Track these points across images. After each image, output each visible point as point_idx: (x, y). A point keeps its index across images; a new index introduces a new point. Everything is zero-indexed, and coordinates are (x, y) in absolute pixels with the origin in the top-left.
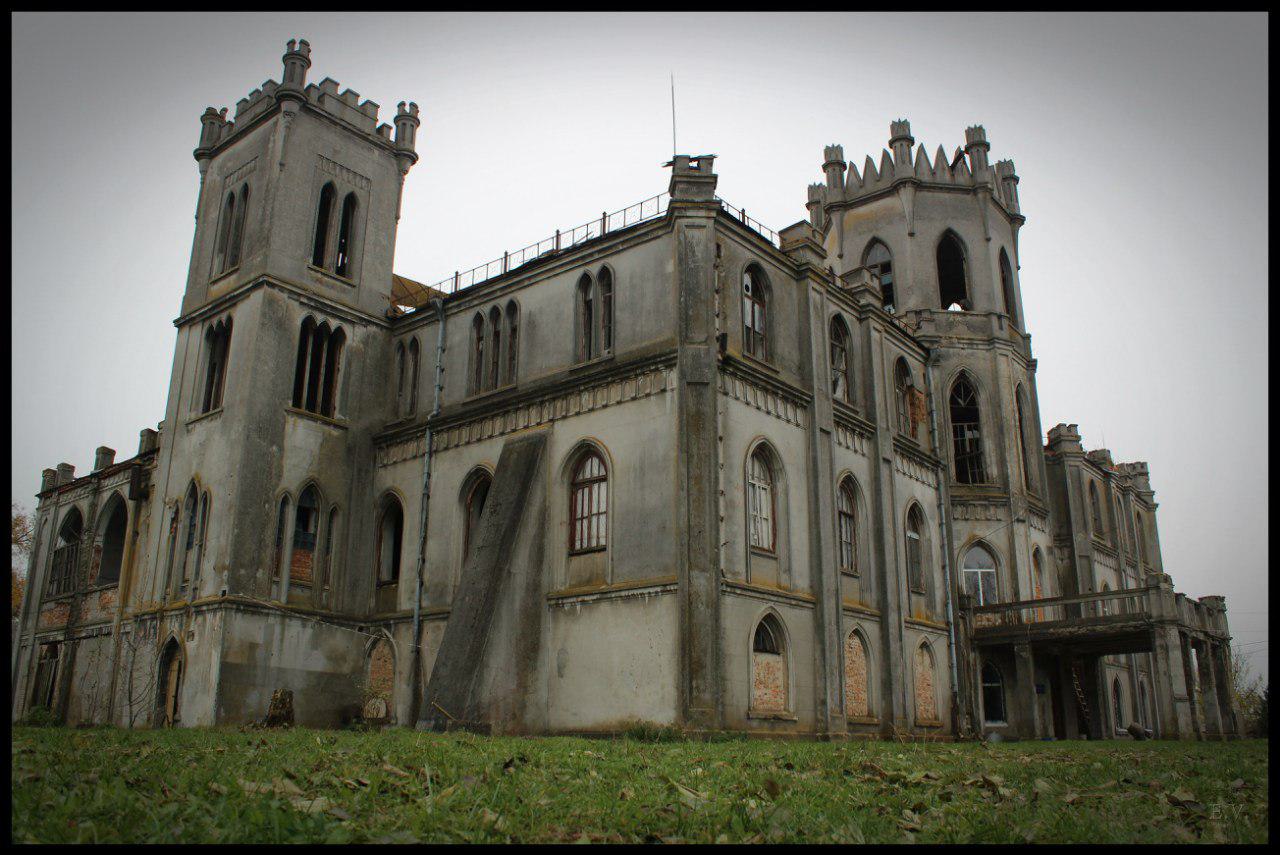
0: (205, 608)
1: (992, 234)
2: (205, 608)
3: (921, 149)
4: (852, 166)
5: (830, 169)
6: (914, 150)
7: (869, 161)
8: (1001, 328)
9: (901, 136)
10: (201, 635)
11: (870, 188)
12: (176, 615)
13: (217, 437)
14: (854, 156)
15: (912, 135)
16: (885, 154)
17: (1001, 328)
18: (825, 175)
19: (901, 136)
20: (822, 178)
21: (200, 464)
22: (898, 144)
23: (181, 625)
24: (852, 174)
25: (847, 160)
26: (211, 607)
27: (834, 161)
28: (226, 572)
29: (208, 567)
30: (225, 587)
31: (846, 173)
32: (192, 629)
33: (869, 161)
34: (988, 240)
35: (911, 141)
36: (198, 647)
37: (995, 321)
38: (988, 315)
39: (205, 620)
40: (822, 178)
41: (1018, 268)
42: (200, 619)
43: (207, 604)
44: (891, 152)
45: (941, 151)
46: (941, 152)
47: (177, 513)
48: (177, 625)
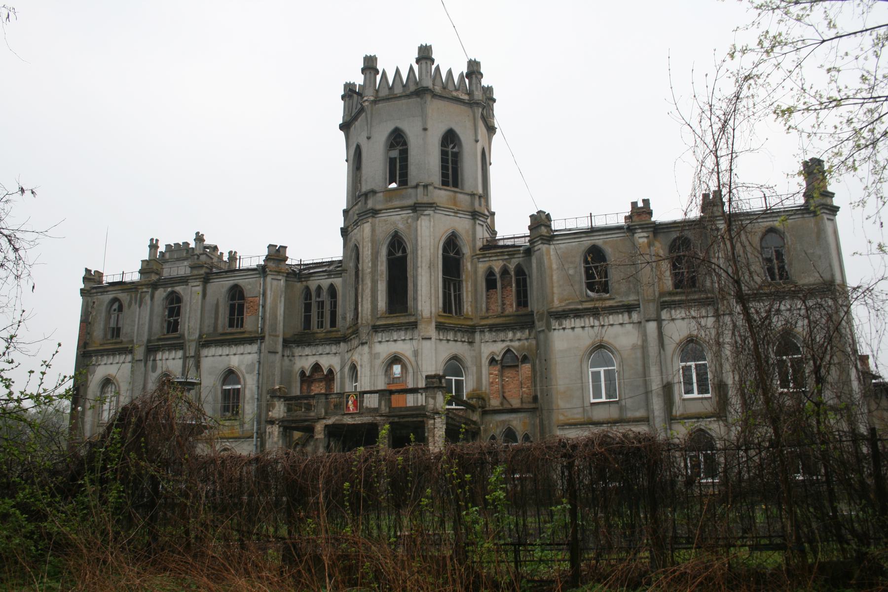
1: (479, 138)
3: (438, 68)
4: (384, 73)
5: (368, 73)
6: (434, 67)
7: (398, 72)
8: (480, 205)
9: (425, 55)
11: (398, 90)
14: (387, 66)
15: (433, 57)
16: (411, 69)
17: (480, 205)
18: (362, 76)
19: (425, 55)
20: (359, 79)
22: (424, 62)
24: (384, 80)
25: (380, 67)
27: (370, 66)
31: (379, 77)
33: (398, 72)
34: (477, 141)
35: (433, 61)
37: (477, 198)
38: (472, 195)
40: (359, 79)
41: (490, 164)
44: (416, 68)
45: (450, 73)
46: (450, 73)
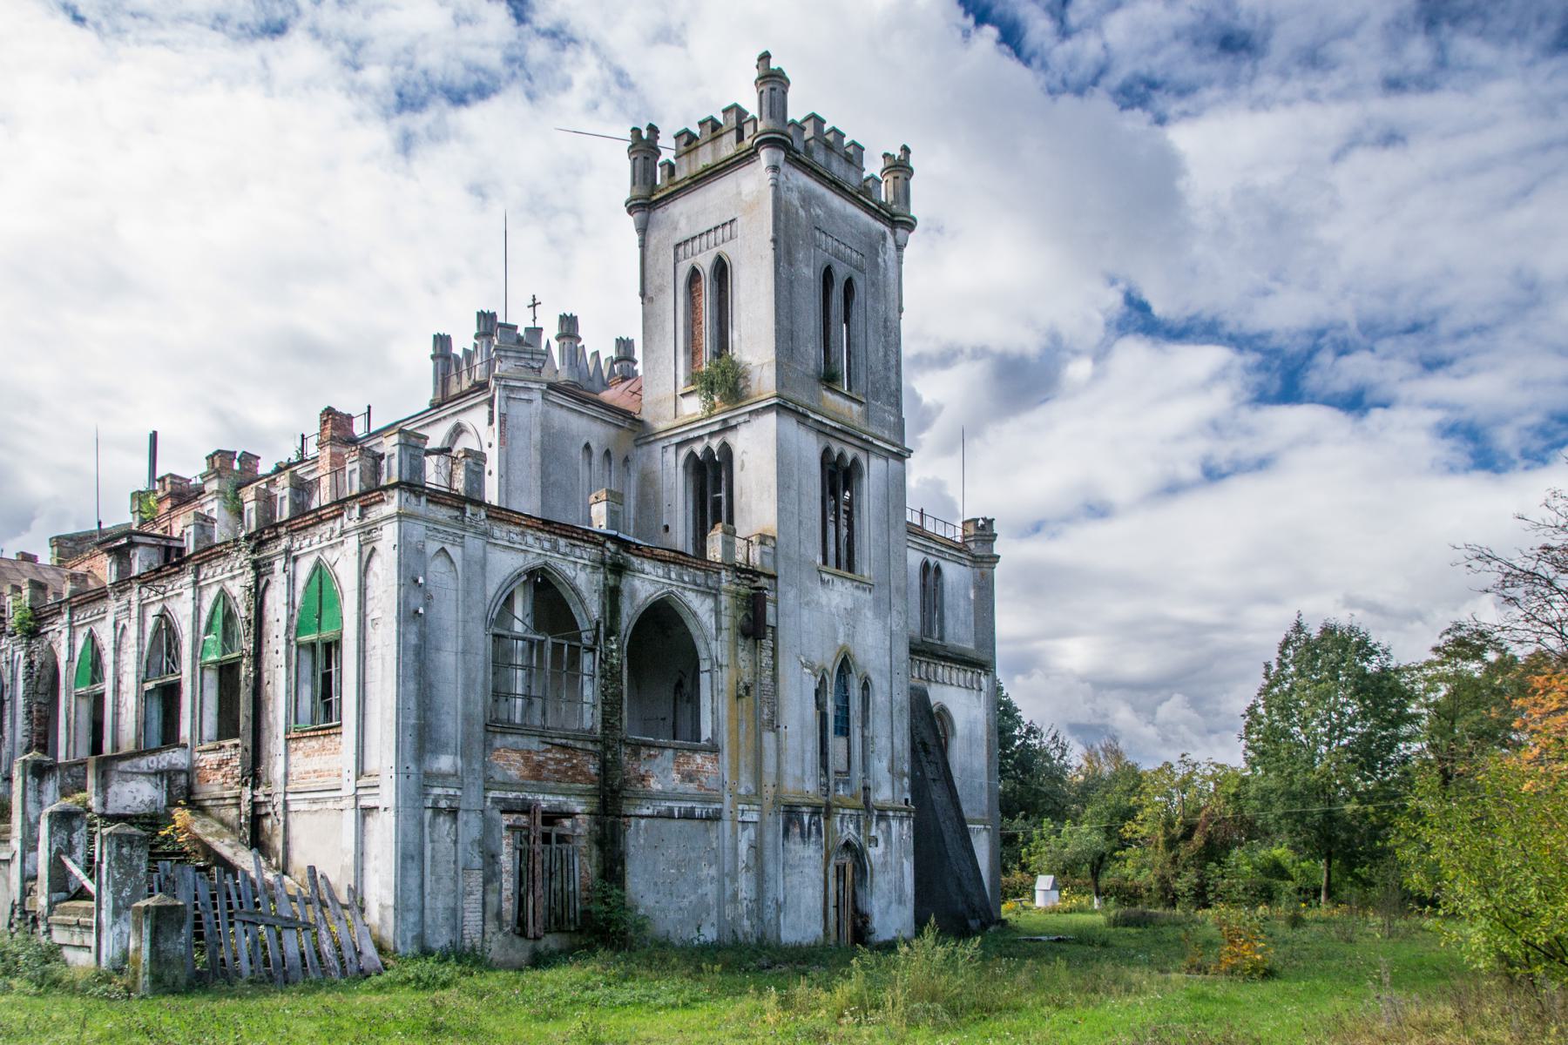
0: (891, 814)
2: (891, 814)
10: (888, 841)
12: (851, 815)
13: (870, 614)
21: (851, 636)
23: (858, 828)
26: (898, 814)
28: (906, 780)
29: (880, 766)
30: (908, 796)
32: (873, 833)
36: (885, 854)
39: (889, 826)
42: (883, 825)
43: (895, 810)
47: (823, 681)
48: (851, 826)
